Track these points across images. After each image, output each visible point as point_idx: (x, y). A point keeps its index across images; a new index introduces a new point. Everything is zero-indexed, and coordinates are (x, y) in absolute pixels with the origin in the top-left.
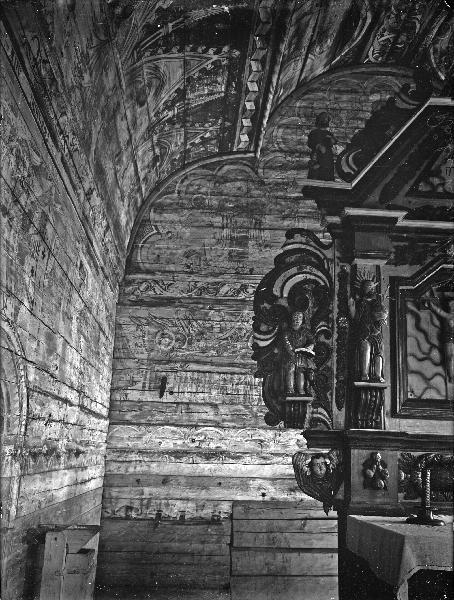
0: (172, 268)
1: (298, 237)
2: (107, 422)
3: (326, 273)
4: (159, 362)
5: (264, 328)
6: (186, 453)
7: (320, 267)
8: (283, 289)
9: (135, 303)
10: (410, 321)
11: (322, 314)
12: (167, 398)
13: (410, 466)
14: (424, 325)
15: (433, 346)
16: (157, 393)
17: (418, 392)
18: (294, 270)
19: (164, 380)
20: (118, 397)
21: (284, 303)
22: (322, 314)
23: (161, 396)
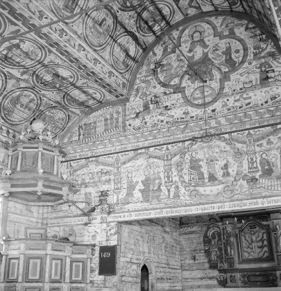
0: (192, 222)
1: (212, 220)
2: (181, 270)
3: (219, 228)
4: (193, 251)
5: (206, 245)
6: (204, 278)
7: (218, 227)
8: (210, 233)
9: (184, 234)
10: (243, 238)
11: (220, 240)
12: (196, 262)
13: (244, 276)
14: (247, 239)
15: (250, 244)
16: (193, 261)
17: (247, 257)
18: (211, 229)
19: (195, 256)
20: (183, 262)
21: (210, 237)
22: (220, 240)
23: (195, 261)
